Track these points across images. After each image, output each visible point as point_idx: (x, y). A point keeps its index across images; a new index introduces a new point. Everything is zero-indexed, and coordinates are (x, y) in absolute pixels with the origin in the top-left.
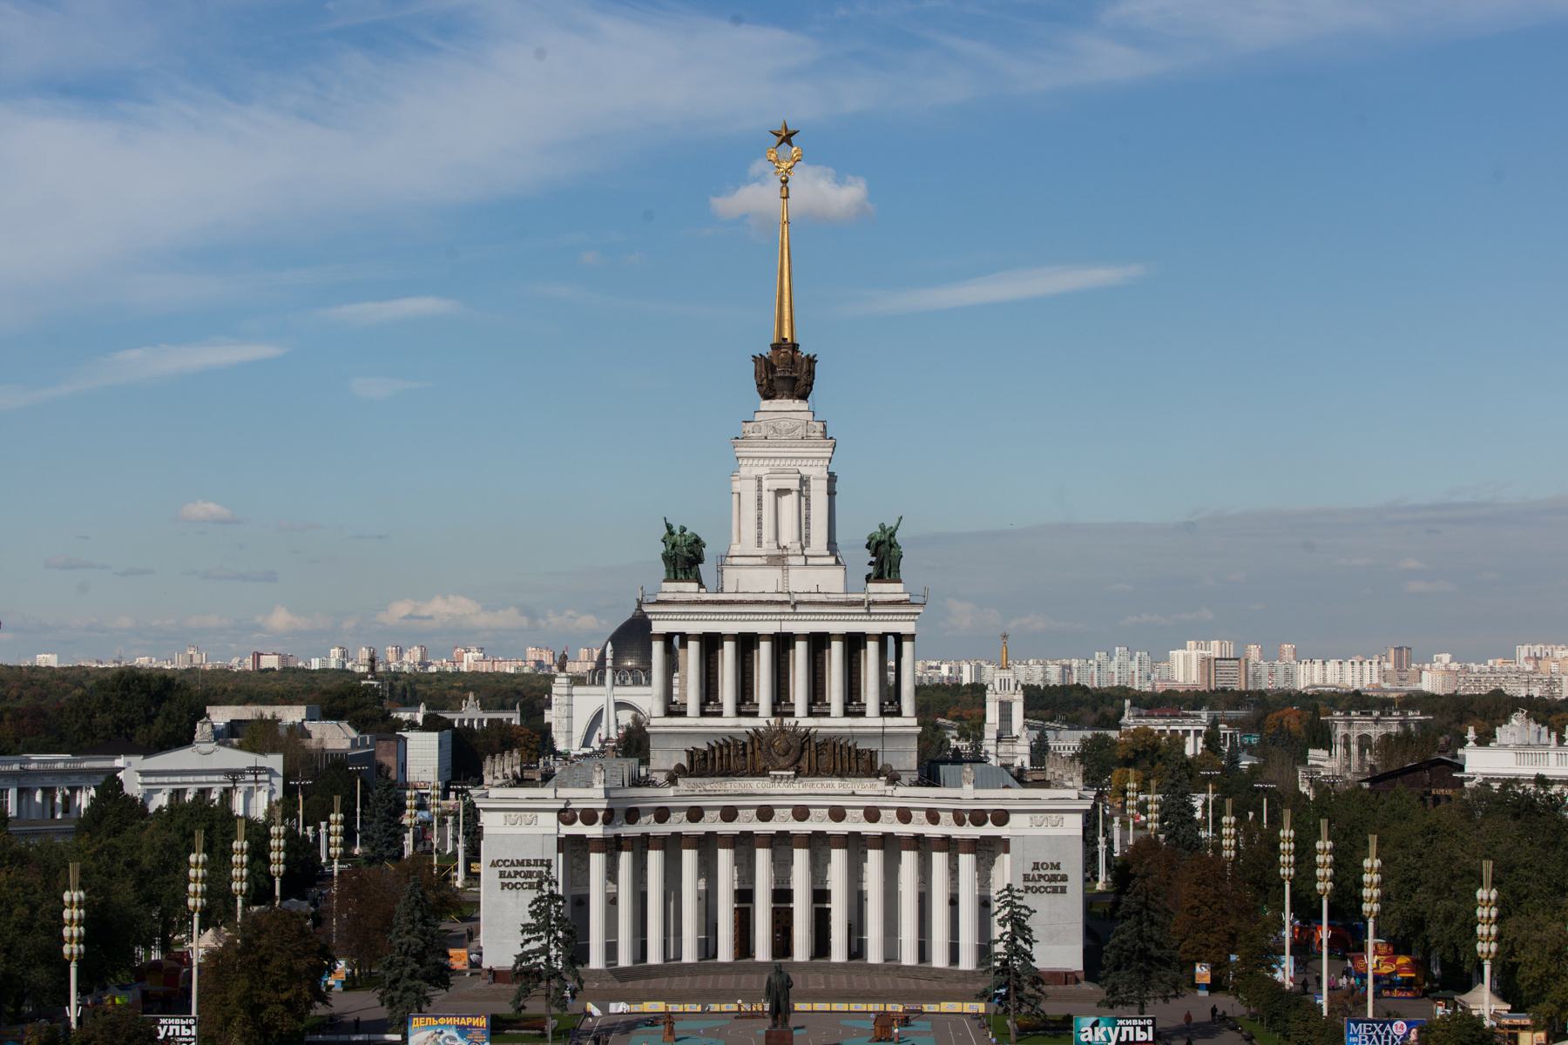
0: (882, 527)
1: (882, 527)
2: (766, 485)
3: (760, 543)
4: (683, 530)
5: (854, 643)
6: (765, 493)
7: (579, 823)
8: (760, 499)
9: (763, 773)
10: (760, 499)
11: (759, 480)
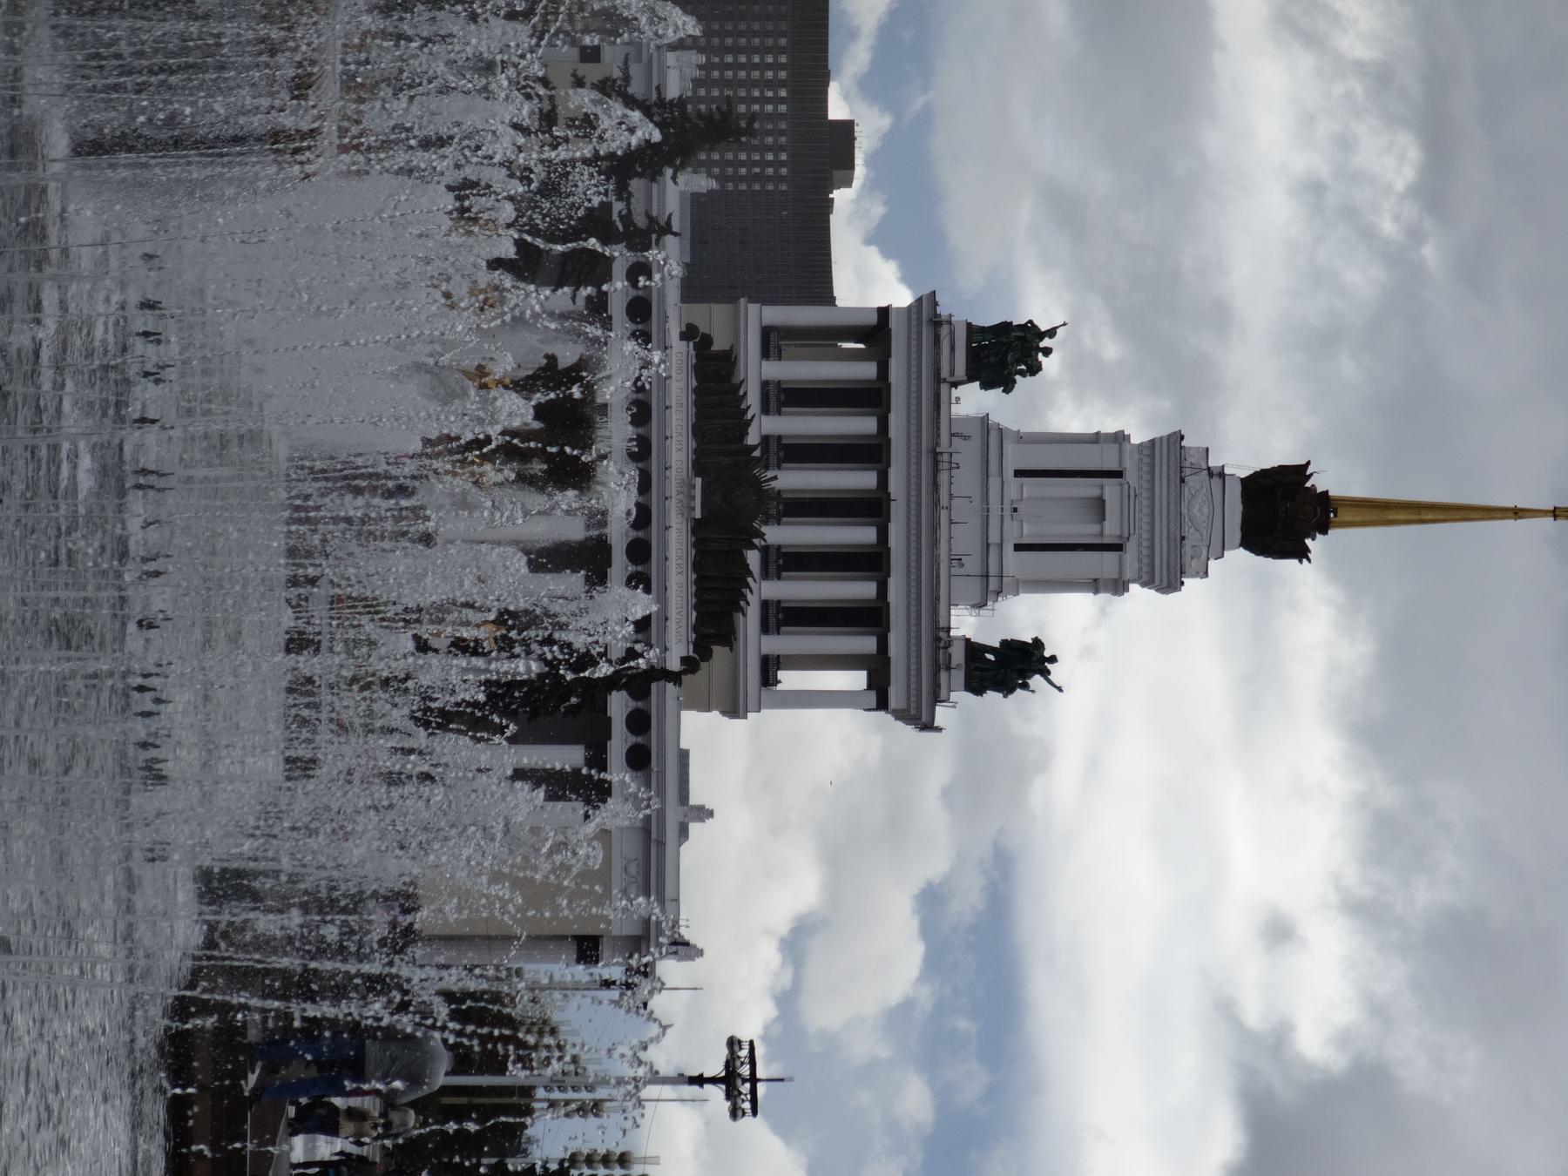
0: (1053, 659)
1: (1053, 659)
3: (1019, 473)
5: (871, 617)
11: (1117, 474)
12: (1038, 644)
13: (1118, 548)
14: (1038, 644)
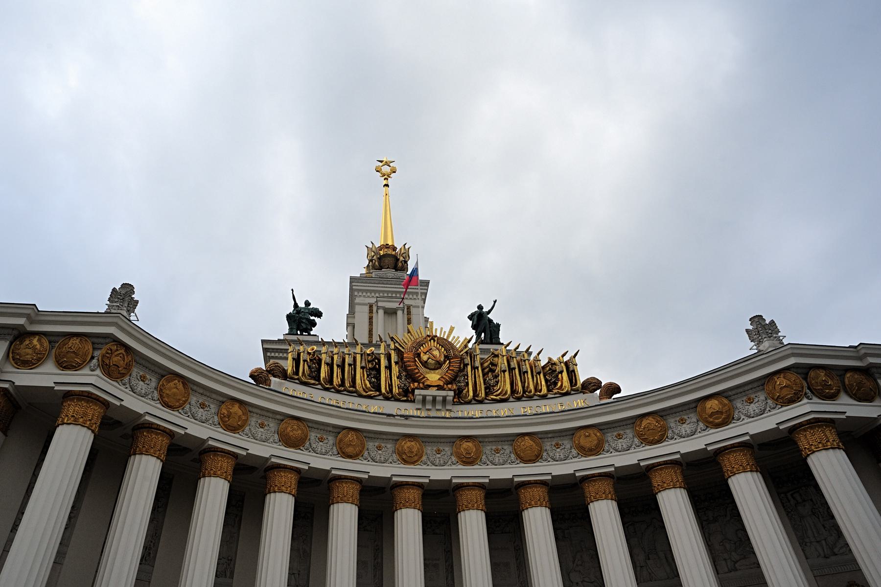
0: (480, 307)
1: (480, 307)
2: (375, 309)
4: (307, 304)
6: (374, 315)
7: (49, 367)
8: (371, 318)
9: (406, 395)
10: (371, 318)
11: (371, 306)
12: (471, 317)
13: (409, 308)
14: (471, 317)
